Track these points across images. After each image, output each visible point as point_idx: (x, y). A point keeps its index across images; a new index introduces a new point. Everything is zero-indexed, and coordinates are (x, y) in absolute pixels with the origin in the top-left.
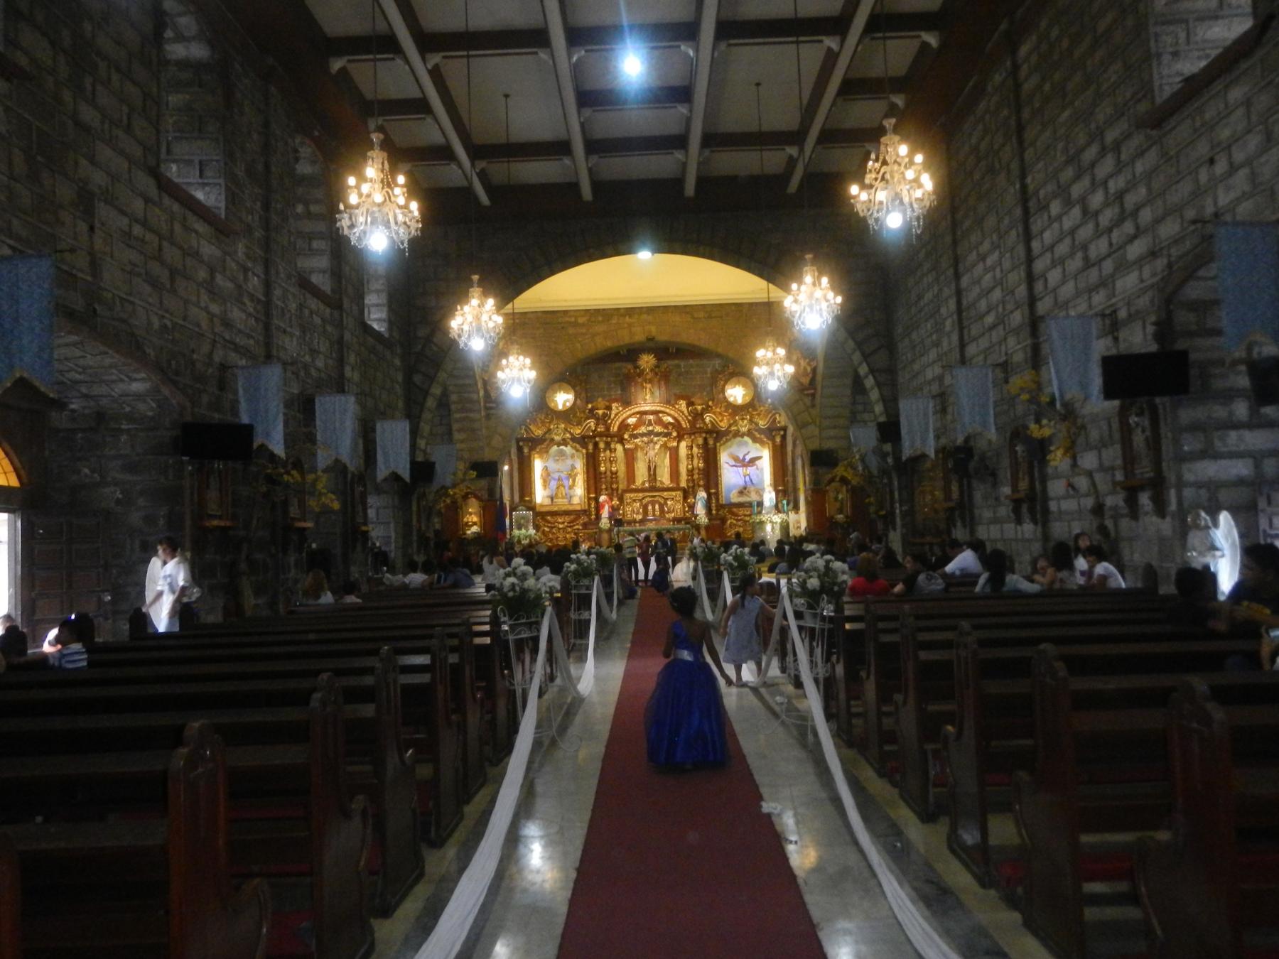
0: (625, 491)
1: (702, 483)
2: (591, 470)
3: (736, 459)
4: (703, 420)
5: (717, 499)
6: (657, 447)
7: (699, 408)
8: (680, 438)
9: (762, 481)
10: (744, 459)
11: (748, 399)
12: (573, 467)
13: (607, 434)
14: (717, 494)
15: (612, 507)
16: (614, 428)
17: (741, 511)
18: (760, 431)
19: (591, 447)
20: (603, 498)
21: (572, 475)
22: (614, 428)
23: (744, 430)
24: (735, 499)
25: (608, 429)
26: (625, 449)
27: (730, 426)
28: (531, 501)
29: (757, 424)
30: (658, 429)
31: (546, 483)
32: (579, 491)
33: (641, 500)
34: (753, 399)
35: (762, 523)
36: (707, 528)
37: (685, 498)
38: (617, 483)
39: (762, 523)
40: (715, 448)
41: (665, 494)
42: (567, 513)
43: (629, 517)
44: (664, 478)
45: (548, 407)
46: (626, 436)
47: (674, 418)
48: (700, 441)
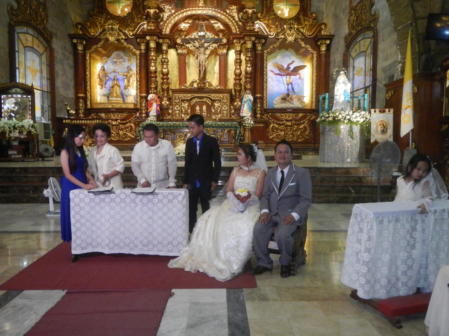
0: (175, 91)
1: (248, 86)
2: (143, 70)
3: (280, 68)
4: (253, 24)
5: (262, 104)
6: (208, 52)
7: (250, 11)
8: (229, 45)
9: (302, 90)
10: (288, 68)
11: (294, 13)
12: (129, 69)
13: (157, 33)
14: (262, 98)
15: (161, 106)
16: (167, 30)
17: (285, 116)
18: (305, 39)
19: (143, 47)
20: (150, 96)
21: (128, 77)
22: (167, 30)
23: (290, 39)
24: (277, 104)
25: (161, 31)
26: (178, 54)
27: (277, 34)
28: (85, 99)
29: (302, 33)
30: (210, 35)
31: (102, 83)
32: (133, 92)
33: (187, 100)
34: (298, 14)
35: (336, 121)
36: (252, 130)
37: (232, 100)
38: (168, 84)
39: (336, 121)
40: (262, 55)
41: (213, 96)
42: (120, 110)
43: (177, 117)
44: (213, 80)
45: (108, 13)
46: (179, 41)
47: (226, 25)
48: (249, 45)
